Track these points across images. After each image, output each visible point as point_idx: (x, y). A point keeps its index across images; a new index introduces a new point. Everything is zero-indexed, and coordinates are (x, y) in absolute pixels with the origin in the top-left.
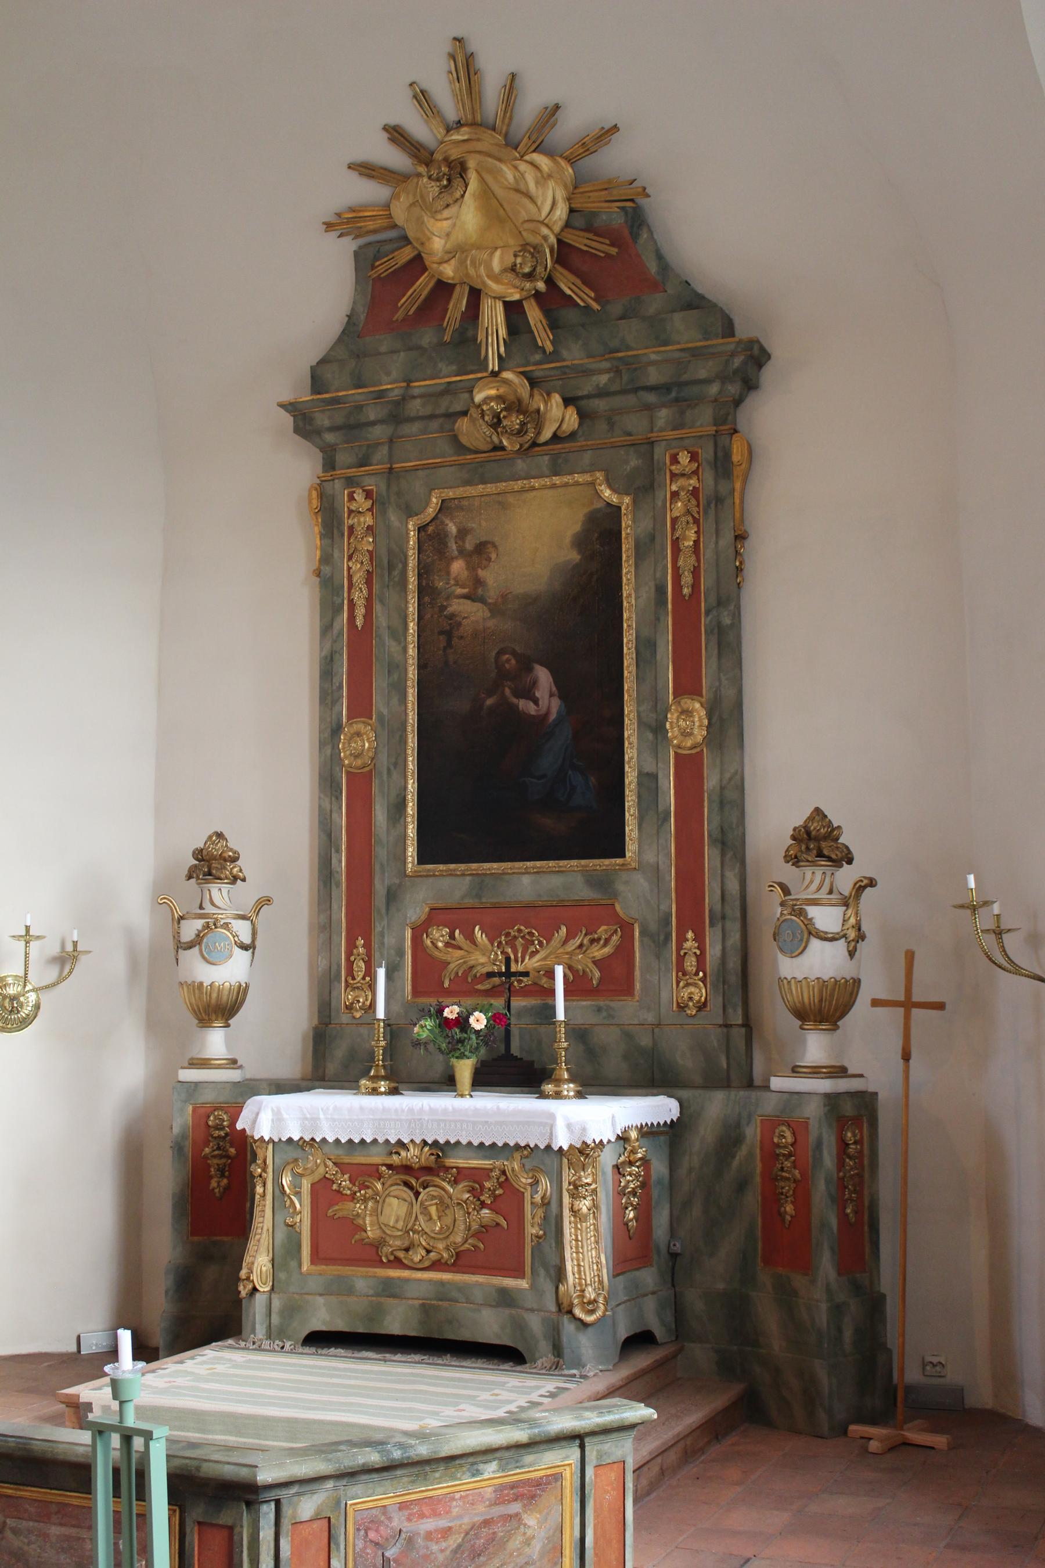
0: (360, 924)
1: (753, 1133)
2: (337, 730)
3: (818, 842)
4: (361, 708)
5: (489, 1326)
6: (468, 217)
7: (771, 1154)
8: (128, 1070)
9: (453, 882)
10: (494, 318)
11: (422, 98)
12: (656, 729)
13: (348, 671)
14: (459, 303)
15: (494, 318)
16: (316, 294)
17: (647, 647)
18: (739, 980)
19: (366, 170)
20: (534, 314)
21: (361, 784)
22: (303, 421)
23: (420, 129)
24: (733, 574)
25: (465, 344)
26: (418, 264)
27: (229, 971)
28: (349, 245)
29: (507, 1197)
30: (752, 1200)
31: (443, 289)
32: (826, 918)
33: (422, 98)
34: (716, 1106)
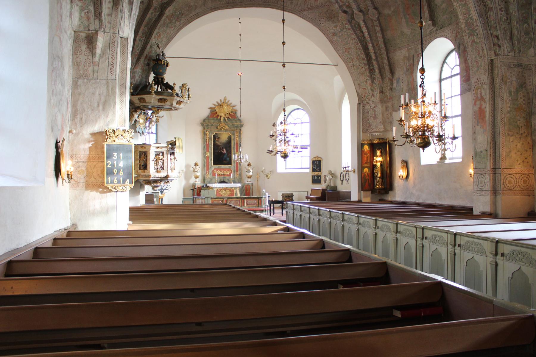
0: (208, 170)
2: (205, 153)
3: (249, 165)
4: (208, 151)
7: (246, 188)
8: (184, 183)
9: (216, 166)
10: (222, 118)
11: (221, 100)
13: (205, 148)
14: (219, 117)
15: (222, 118)
16: (206, 113)
17: (234, 148)
18: (240, 175)
19: (214, 105)
21: (208, 158)
22: (202, 124)
23: (220, 102)
28: (209, 110)
29: (233, 191)
30: (245, 191)
31: (218, 115)
32: (251, 170)
33: (221, 100)
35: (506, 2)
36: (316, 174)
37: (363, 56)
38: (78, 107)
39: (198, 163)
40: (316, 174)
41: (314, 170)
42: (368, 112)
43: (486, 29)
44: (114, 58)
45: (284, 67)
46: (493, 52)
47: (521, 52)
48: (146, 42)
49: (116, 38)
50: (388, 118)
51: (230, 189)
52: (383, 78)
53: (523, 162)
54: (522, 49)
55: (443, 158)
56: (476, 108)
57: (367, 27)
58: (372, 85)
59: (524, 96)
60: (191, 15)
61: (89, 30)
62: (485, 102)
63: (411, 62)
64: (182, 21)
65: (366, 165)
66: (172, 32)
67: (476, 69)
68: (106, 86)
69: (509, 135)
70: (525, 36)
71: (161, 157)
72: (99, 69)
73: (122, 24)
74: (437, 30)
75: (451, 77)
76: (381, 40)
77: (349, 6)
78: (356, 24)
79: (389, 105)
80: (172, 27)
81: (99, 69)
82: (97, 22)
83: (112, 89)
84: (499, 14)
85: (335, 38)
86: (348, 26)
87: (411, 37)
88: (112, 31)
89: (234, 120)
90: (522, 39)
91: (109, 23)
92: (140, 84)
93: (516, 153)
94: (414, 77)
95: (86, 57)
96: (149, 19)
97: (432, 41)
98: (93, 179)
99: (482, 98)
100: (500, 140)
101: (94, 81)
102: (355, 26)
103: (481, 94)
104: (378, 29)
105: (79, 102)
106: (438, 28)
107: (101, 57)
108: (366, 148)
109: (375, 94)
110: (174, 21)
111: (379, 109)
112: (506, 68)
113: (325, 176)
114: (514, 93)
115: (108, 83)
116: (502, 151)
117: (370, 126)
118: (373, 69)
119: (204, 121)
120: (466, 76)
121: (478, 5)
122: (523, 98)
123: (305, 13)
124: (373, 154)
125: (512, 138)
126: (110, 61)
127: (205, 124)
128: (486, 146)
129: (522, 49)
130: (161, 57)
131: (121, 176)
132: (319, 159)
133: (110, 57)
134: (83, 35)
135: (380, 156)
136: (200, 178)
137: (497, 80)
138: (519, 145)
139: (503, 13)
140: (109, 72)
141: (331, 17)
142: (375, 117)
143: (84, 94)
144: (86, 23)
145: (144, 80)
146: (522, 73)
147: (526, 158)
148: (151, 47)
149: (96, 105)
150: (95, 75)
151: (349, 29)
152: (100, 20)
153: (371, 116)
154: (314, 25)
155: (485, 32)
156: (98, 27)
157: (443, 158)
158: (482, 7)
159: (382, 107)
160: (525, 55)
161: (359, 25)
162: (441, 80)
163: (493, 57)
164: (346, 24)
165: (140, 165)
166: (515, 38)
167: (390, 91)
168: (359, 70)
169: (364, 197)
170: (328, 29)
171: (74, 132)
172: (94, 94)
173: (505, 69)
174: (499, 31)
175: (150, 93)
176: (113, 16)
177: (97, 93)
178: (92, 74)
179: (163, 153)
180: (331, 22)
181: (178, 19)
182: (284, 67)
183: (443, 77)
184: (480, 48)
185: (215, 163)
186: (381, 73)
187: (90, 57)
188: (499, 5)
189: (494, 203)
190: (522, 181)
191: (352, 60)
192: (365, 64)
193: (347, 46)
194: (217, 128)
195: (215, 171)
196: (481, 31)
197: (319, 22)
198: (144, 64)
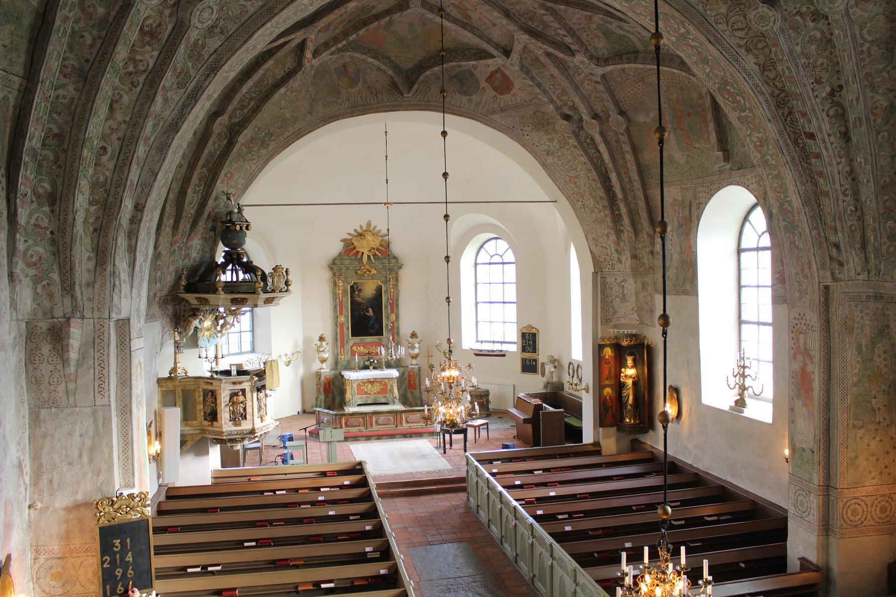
0: (342, 346)
1: (406, 373)
3: (414, 335)
4: (341, 313)
5: (383, 401)
6: (365, 243)
7: (409, 375)
8: (301, 371)
9: (357, 339)
11: (361, 227)
12: (388, 318)
13: (337, 309)
14: (360, 254)
16: (336, 248)
17: (386, 306)
20: (372, 257)
22: (331, 269)
23: (360, 231)
24: (398, 295)
25: (361, 259)
26: (355, 248)
27: (326, 355)
28: (342, 244)
29: (386, 384)
30: (407, 382)
31: (358, 252)
32: (417, 345)
33: (361, 227)
34: (402, 369)
35: (853, 180)
36: (528, 355)
37: (601, 193)
38: (43, 460)
39: (325, 336)
40: (528, 355)
41: (524, 349)
42: (611, 289)
43: (816, 228)
44: (103, 365)
45: (448, 262)
46: (829, 273)
47: (881, 273)
48: (207, 193)
49: (106, 326)
50: (647, 303)
51: (381, 381)
52: (636, 231)
53: (881, 473)
54: (882, 267)
55: (740, 403)
56: (797, 366)
57: (607, 143)
58: (617, 244)
59: (885, 352)
60: (288, 134)
61: (53, 318)
62: (812, 362)
63: (687, 212)
64: (271, 147)
65: (607, 382)
66: (253, 167)
67: (797, 294)
68: (92, 419)
69: (854, 426)
70: (889, 243)
71: (241, 398)
72: (76, 388)
73: (116, 298)
74: (731, 169)
75: (758, 249)
76: (632, 167)
77: (574, 108)
78: (587, 137)
79: (648, 279)
80: (253, 159)
81: (76, 388)
82: (67, 301)
83: (104, 423)
84: (840, 202)
85: (550, 159)
86: (573, 141)
87: (686, 169)
88: (96, 314)
89: (386, 259)
90: (884, 248)
91: (90, 300)
92: (201, 263)
93: (867, 459)
94: (692, 243)
95: (52, 368)
96: (210, 153)
97: (723, 187)
98: (78, 586)
99: (807, 352)
100: (838, 437)
101: (69, 411)
102: (585, 141)
103: (805, 344)
104: (627, 148)
105: (45, 450)
106: (732, 164)
107: (79, 365)
108: (608, 352)
109: (623, 258)
110: (255, 149)
111: (631, 286)
112: (853, 304)
113: (543, 364)
114: (867, 348)
115: (95, 413)
116: (841, 456)
117: (615, 312)
118: (620, 215)
119: (334, 263)
120: (780, 278)
121: (803, 183)
122: (883, 356)
123: (495, 117)
124: (621, 364)
125: (860, 432)
126: (97, 372)
127: (336, 266)
128: (812, 443)
129: (882, 267)
130: (235, 217)
131: (130, 579)
132: (534, 331)
133: (96, 364)
134: (44, 325)
135: (632, 367)
136: (330, 361)
137: (836, 326)
138: (873, 444)
139: (848, 199)
140: (97, 391)
141: (541, 123)
142: (624, 299)
143: (53, 436)
144: (47, 304)
145: (208, 255)
146: (883, 309)
147: (886, 467)
148: (217, 198)
149: (76, 454)
150: (71, 398)
151: (575, 147)
152: (73, 297)
153: (617, 296)
154: (512, 138)
155: (814, 233)
156: (69, 310)
157: (740, 403)
158: (809, 185)
159: (636, 283)
160: (889, 279)
161: (592, 139)
162: (739, 251)
163: (829, 281)
164: (569, 138)
165: (205, 413)
166: (870, 248)
167: (651, 257)
168: (594, 215)
169: (604, 438)
170: (537, 144)
171: (39, 505)
172: (70, 434)
173: (850, 306)
174: (840, 235)
175: (214, 291)
176: (97, 286)
177: (77, 433)
178: (64, 398)
179: (243, 391)
180: (542, 133)
181: (264, 144)
182: (448, 262)
183: (743, 246)
184: (805, 260)
185: (354, 334)
186: (634, 224)
187: (60, 367)
188: (841, 185)
189: (825, 548)
190: (878, 509)
191: (582, 197)
192: (604, 207)
193: (572, 173)
194: (356, 273)
195: (355, 348)
196: (807, 231)
197: (521, 133)
198: (205, 229)
